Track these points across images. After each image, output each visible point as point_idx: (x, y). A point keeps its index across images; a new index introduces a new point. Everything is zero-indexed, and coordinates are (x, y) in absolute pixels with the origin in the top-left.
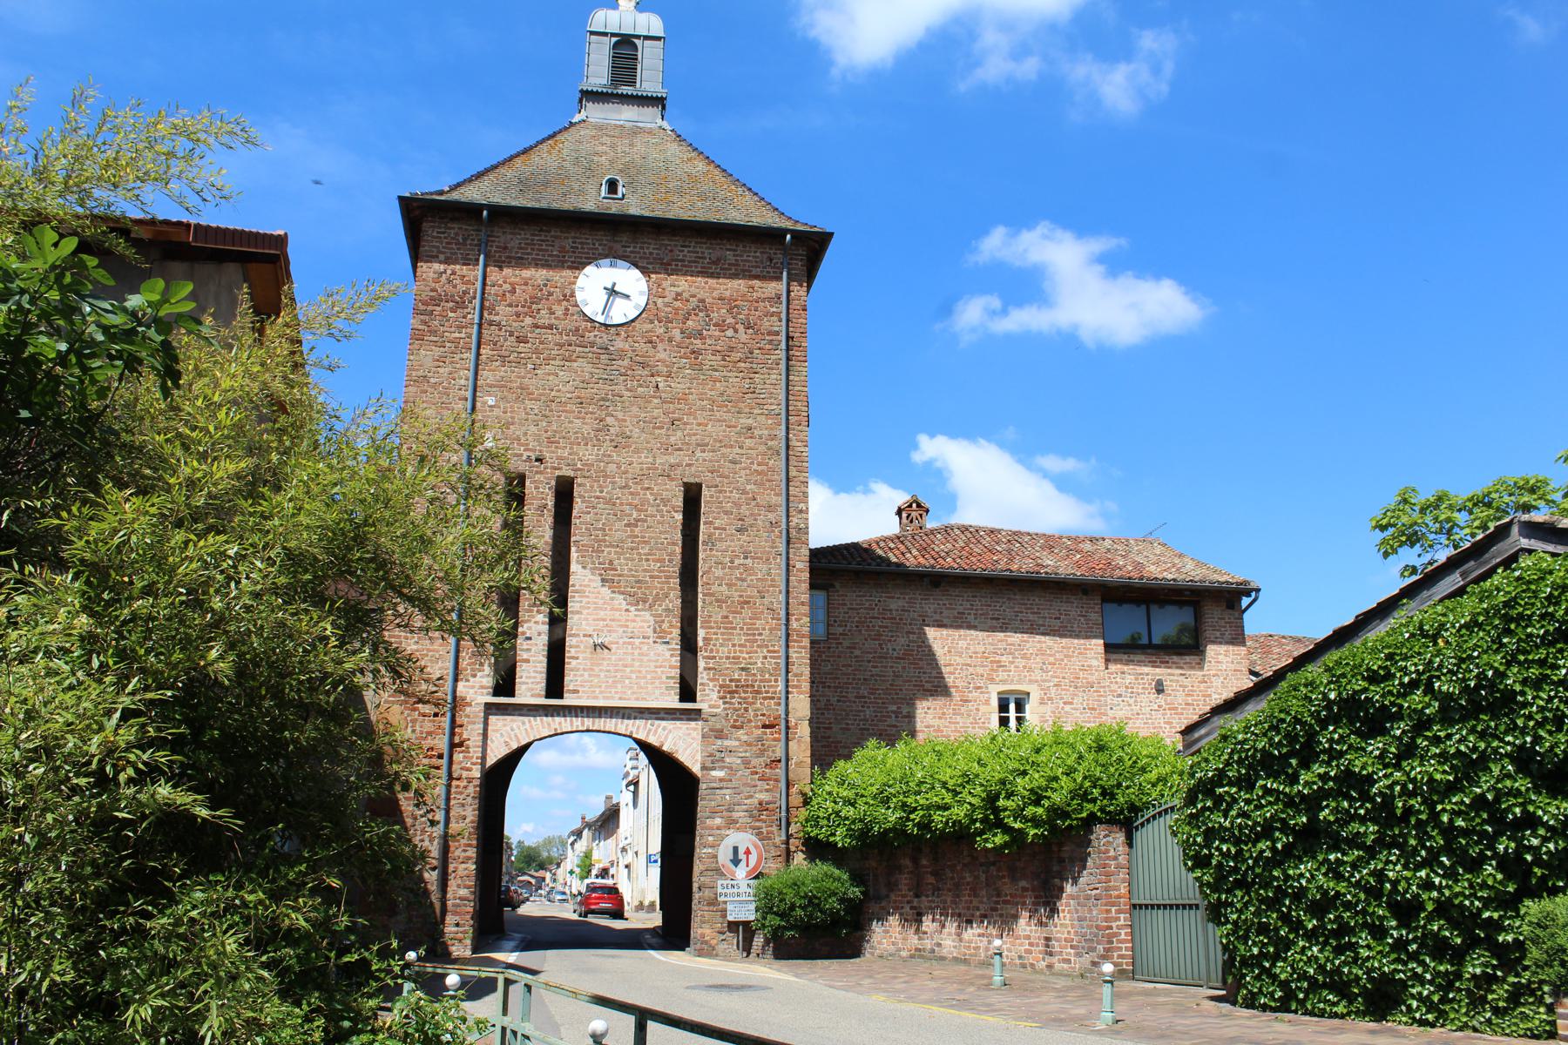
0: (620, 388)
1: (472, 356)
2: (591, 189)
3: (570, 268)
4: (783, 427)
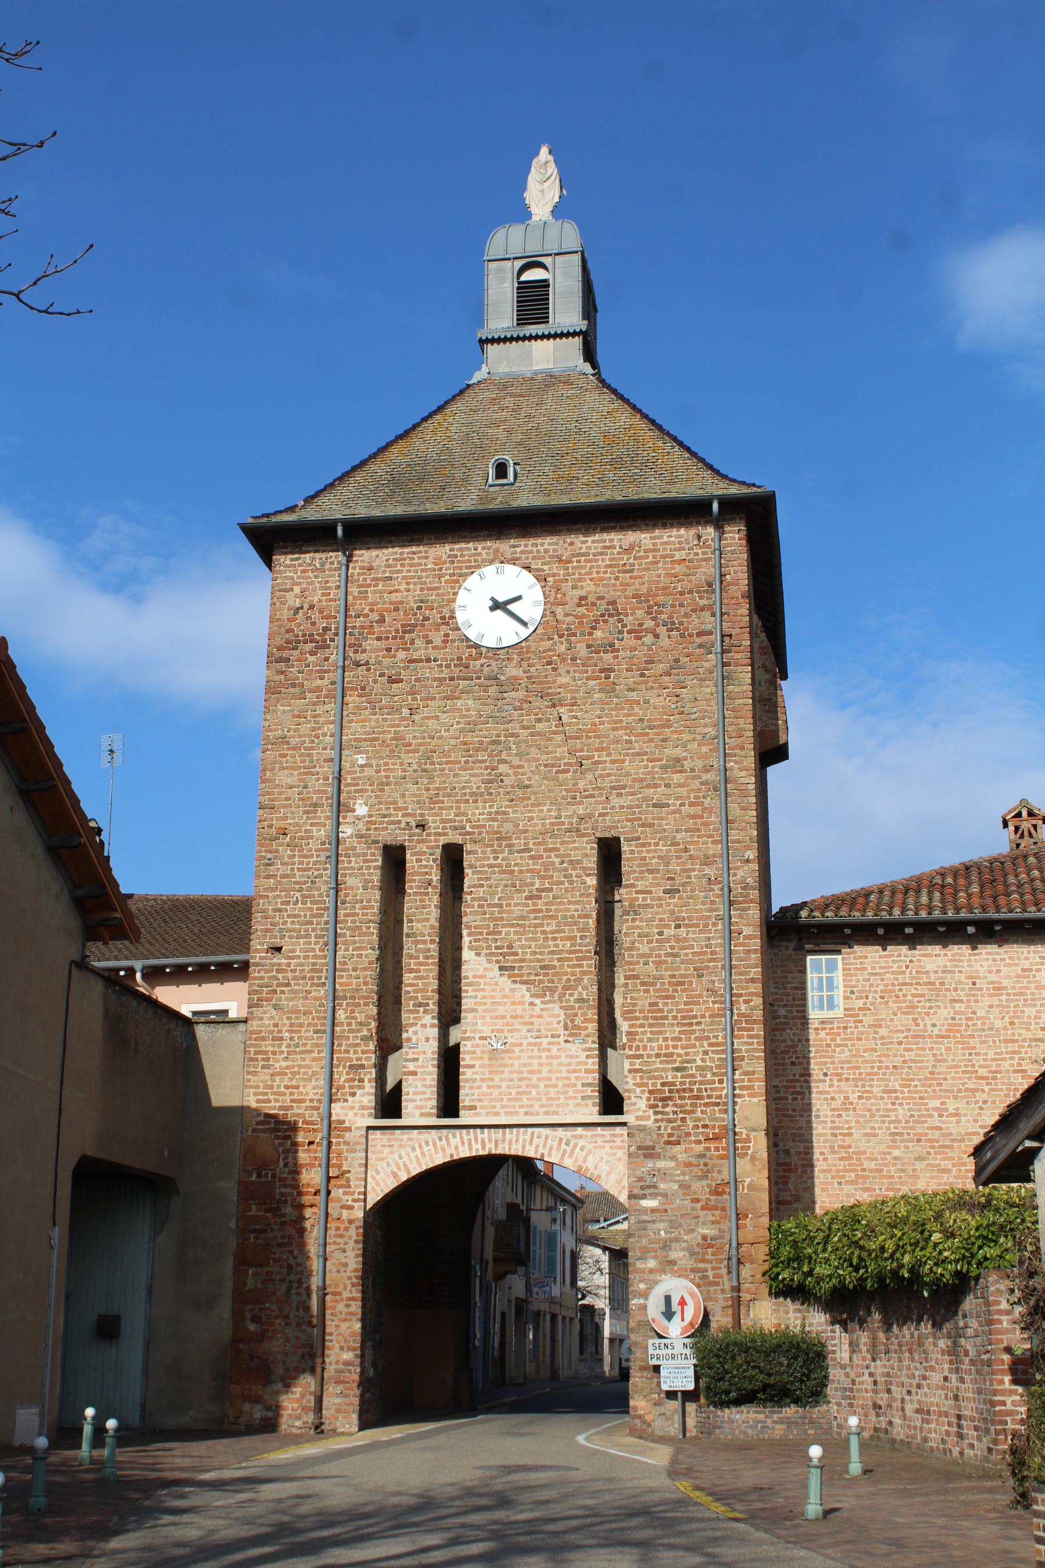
0: (514, 727)
2: (477, 479)
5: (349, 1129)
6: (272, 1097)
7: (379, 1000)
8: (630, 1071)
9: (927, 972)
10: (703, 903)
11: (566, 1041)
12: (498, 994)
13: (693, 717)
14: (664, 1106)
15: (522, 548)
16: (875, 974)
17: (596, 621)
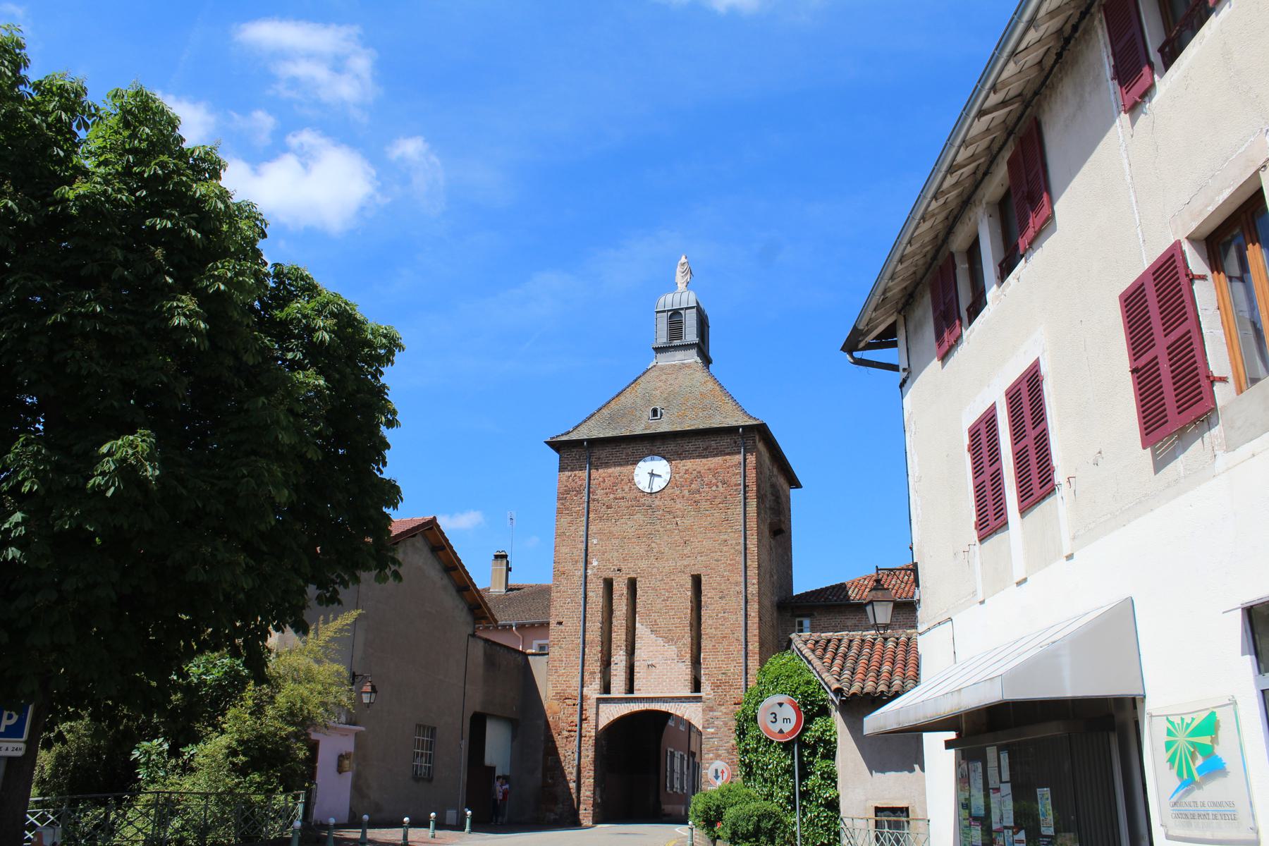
1: (584, 519)
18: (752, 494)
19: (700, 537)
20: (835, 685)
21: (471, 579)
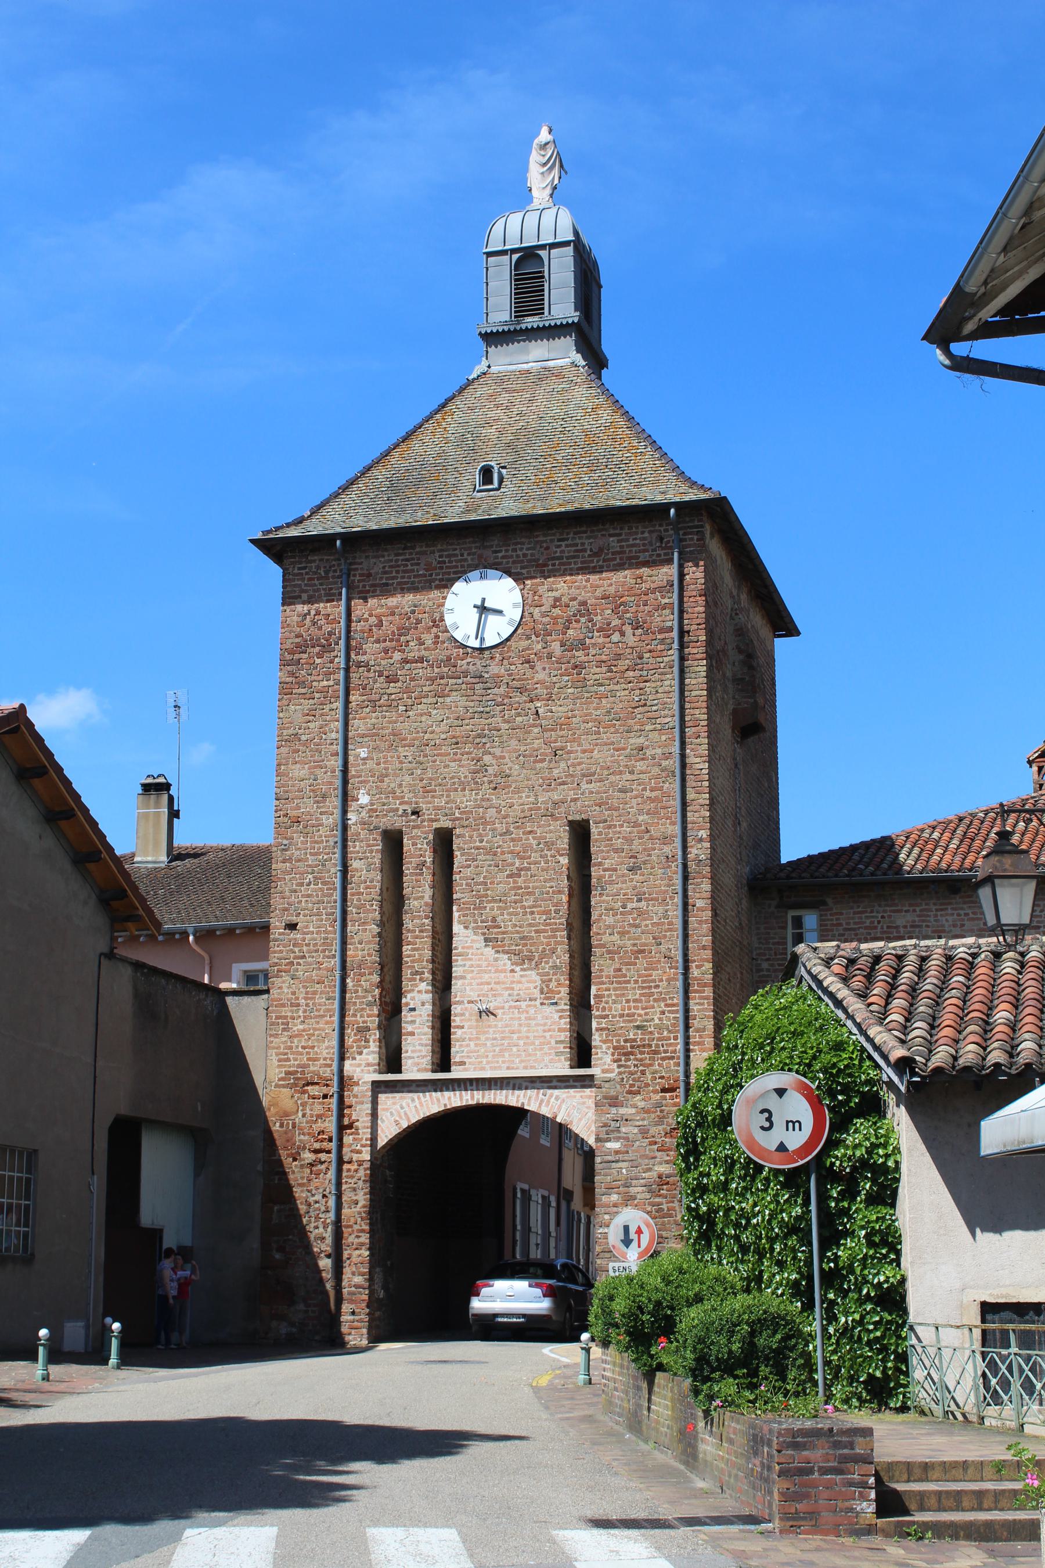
3: (438, 587)
4: (677, 743)
5: (357, 1084)
6: (291, 1057)
7: (382, 969)
8: (597, 1030)
9: (897, 927)
10: (662, 879)
11: (542, 1004)
12: (485, 964)
13: (654, 708)
14: (627, 1060)
15: (503, 553)
16: (850, 929)
17: (569, 621)
18: (697, 650)
19: (586, 742)
20: (899, 1052)
21: (102, 837)
